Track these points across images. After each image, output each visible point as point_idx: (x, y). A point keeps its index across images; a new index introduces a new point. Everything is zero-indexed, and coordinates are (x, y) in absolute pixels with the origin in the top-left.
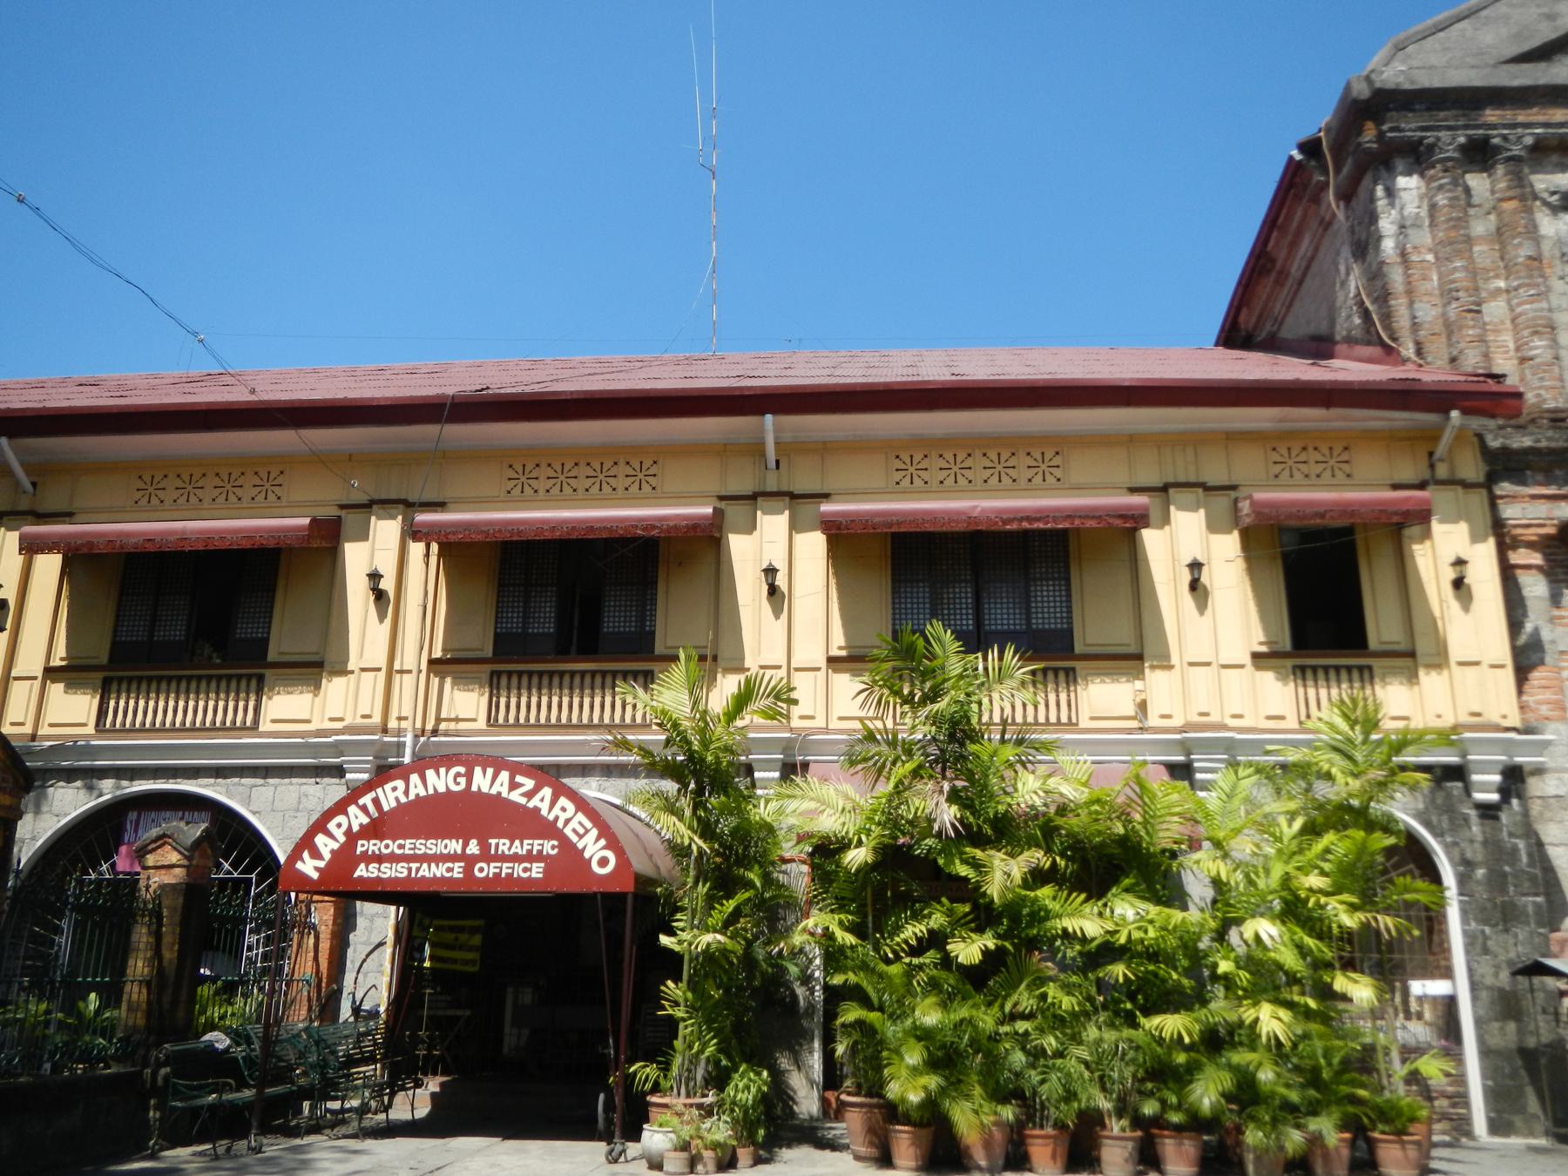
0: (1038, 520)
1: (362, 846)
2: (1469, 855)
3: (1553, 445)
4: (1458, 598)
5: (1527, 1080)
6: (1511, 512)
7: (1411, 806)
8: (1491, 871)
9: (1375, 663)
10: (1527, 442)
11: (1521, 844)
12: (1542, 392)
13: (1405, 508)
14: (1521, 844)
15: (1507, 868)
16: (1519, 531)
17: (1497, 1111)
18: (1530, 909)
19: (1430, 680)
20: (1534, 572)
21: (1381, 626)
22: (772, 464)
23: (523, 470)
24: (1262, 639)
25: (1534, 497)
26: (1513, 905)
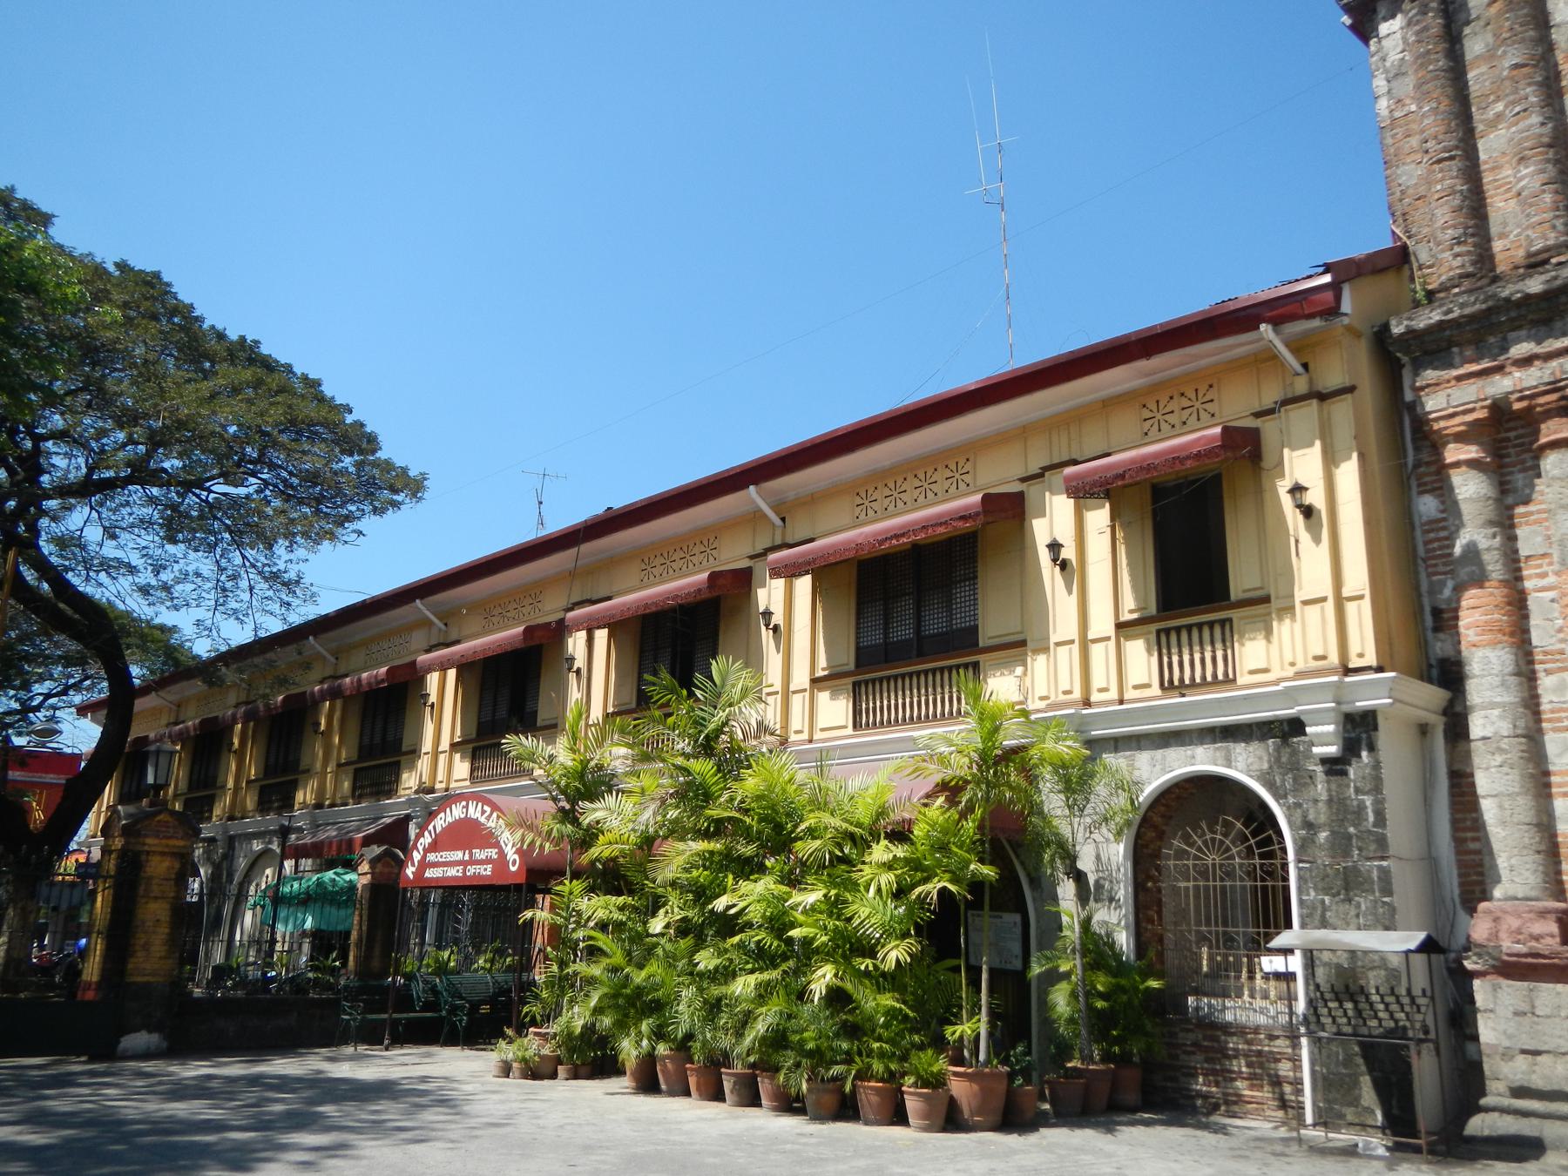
0: (903, 535)
1: (431, 857)
2: (1311, 817)
3: (1467, 311)
4: (1308, 528)
5: (1363, 1068)
6: (1433, 403)
7: (1256, 767)
8: (1333, 833)
9: (1234, 614)
10: (1436, 316)
11: (1368, 801)
12: (1529, 232)
13: (1195, 451)
14: (1368, 801)
15: (1352, 830)
16: (1442, 424)
17: (1326, 1101)
18: (1375, 874)
19: (1283, 629)
20: (1464, 468)
21: (1242, 578)
22: (778, 522)
23: (649, 559)
24: (1133, 607)
25: (1459, 379)
26: (1355, 869)
